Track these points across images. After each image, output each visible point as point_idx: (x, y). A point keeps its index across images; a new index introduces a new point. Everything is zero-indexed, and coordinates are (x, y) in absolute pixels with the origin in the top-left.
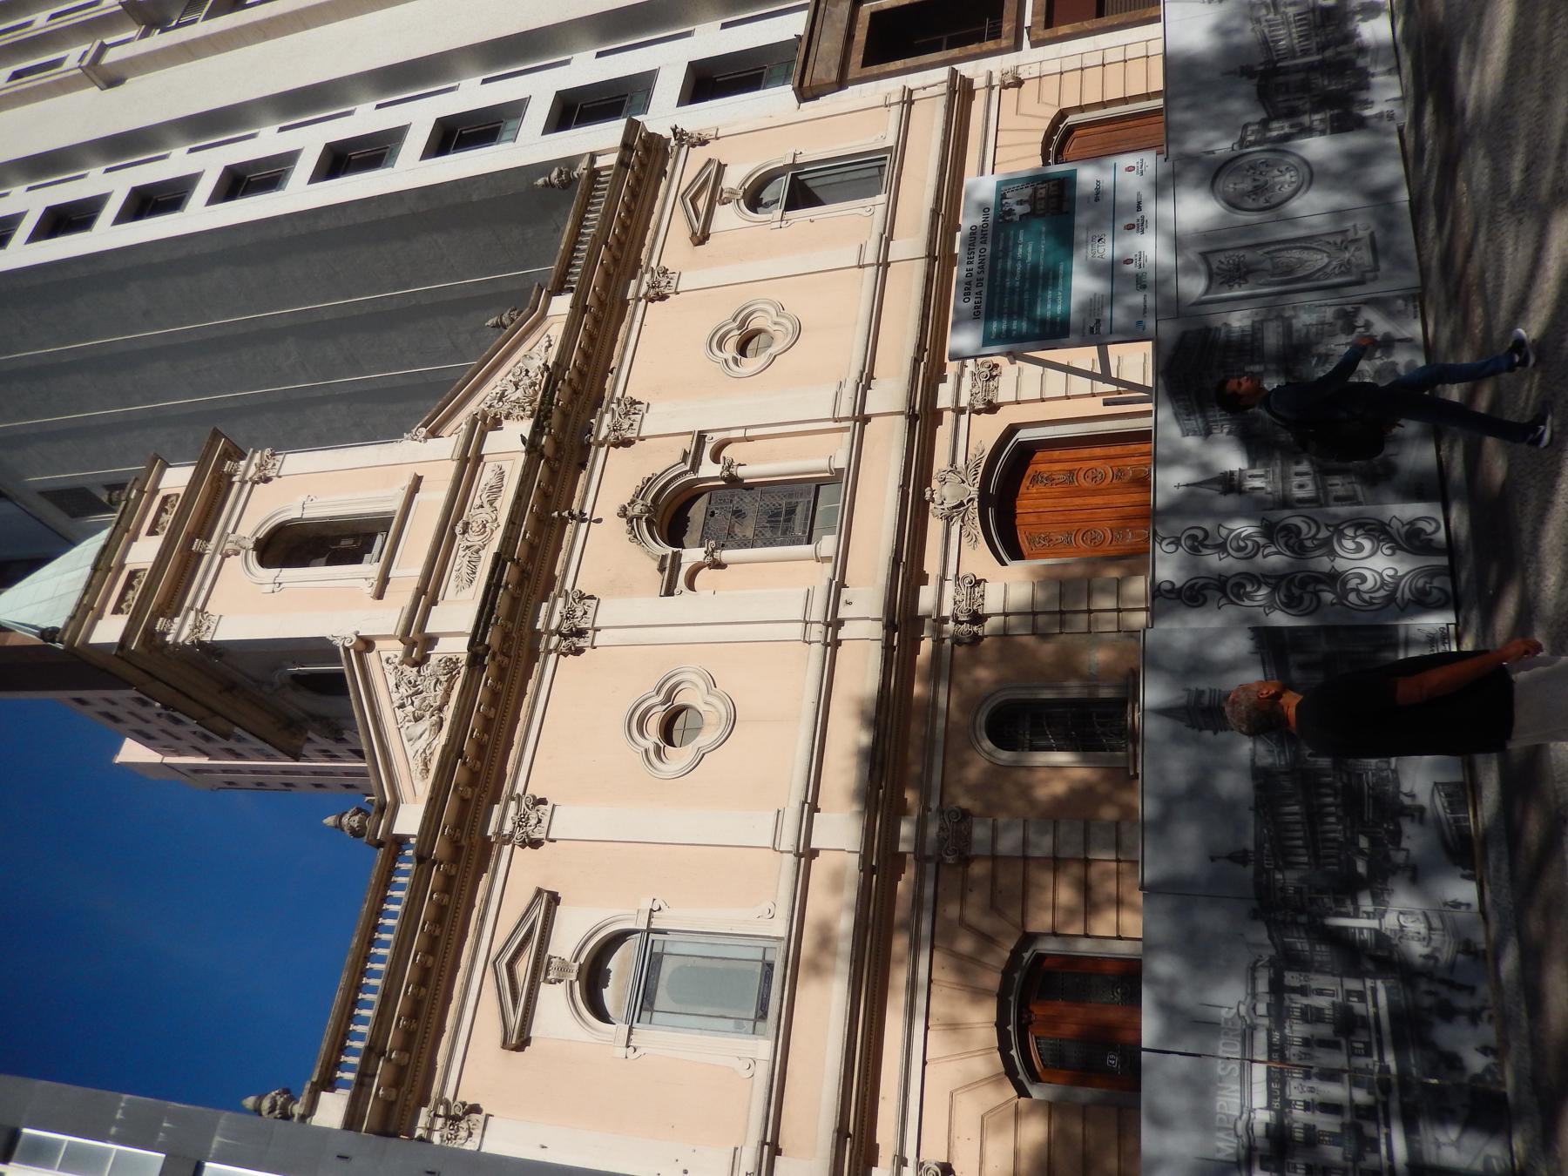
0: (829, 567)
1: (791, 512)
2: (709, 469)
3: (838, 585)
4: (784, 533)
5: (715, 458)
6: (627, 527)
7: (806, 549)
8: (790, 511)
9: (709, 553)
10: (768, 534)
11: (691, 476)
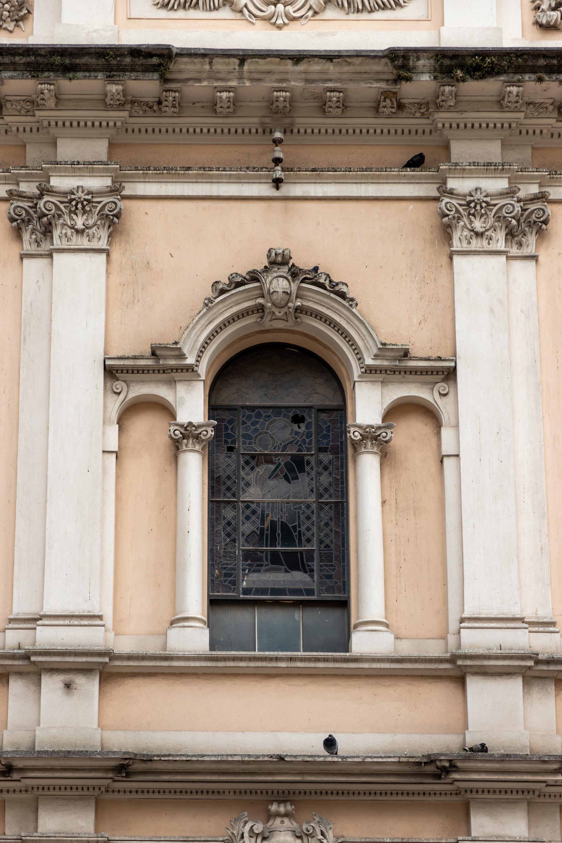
0: (152, 647)
1: (294, 562)
2: (367, 406)
3: (108, 669)
4: (248, 555)
5: (397, 411)
6: (243, 271)
7: (195, 600)
8: (282, 559)
9: (189, 432)
10: (247, 528)
11: (356, 371)
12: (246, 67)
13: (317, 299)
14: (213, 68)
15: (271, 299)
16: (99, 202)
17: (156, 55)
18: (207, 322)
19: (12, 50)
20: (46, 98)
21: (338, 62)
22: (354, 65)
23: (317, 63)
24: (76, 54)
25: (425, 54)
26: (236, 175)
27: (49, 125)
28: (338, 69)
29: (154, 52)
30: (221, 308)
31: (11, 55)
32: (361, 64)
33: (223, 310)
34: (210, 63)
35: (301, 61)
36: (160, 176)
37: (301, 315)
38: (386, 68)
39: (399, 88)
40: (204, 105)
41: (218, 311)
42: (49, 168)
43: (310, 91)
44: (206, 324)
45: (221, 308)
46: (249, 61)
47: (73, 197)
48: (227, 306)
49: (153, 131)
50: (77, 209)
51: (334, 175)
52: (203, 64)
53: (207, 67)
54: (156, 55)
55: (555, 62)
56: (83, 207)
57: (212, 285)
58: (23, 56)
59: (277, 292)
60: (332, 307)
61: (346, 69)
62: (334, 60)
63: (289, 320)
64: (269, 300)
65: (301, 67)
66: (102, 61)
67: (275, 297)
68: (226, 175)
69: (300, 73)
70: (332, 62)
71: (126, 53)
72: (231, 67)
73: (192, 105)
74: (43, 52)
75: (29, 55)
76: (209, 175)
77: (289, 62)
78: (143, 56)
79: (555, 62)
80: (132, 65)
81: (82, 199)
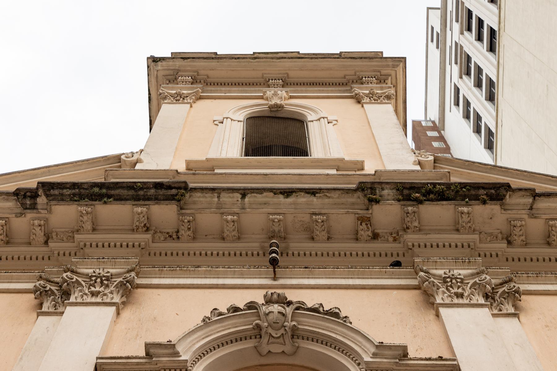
12: (247, 199)
13: (313, 323)
14: (221, 200)
15: (267, 320)
16: (115, 281)
17: (175, 188)
18: (204, 336)
19: (61, 185)
20: (84, 221)
21: (320, 197)
22: (333, 198)
23: (304, 197)
24: (111, 188)
25: (388, 186)
26: (239, 271)
27: (85, 245)
28: (320, 200)
29: (173, 186)
30: (219, 327)
31: (60, 188)
32: (338, 198)
33: (221, 329)
34: (219, 197)
35: (290, 195)
36: (174, 272)
37: (298, 340)
38: (359, 200)
39: (371, 214)
40: (215, 236)
41: (215, 329)
42: (77, 262)
43: (299, 219)
44: (203, 337)
45: (219, 327)
46: (249, 195)
47: (94, 274)
48: (225, 326)
49: (172, 254)
50: (96, 282)
51: (324, 271)
52: (212, 197)
53: (216, 199)
54: (175, 188)
55: (493, 191)
56: (102, 282)
57: (211, 312)
58: (70, 189)
59: (273, 312)
60: (328, 327)
61: (327, 201)
62: (317, 195)
63: (286, 343)
64: (265, 321)
65: (290, 200)
66: (131, 192)
67: (271, 317)
68: (231, 271)
69: (291, 204)
70: (315, 196)
71: (151, 186)
72: (236, 199)
73: (204, 237)
74: (86, 186)
75: (74, 189)
76: (216, 271)
77: (281, 196)
78: (165, 188)
79: (493, 191)
80: (155, 195)
81: (101, 275)
